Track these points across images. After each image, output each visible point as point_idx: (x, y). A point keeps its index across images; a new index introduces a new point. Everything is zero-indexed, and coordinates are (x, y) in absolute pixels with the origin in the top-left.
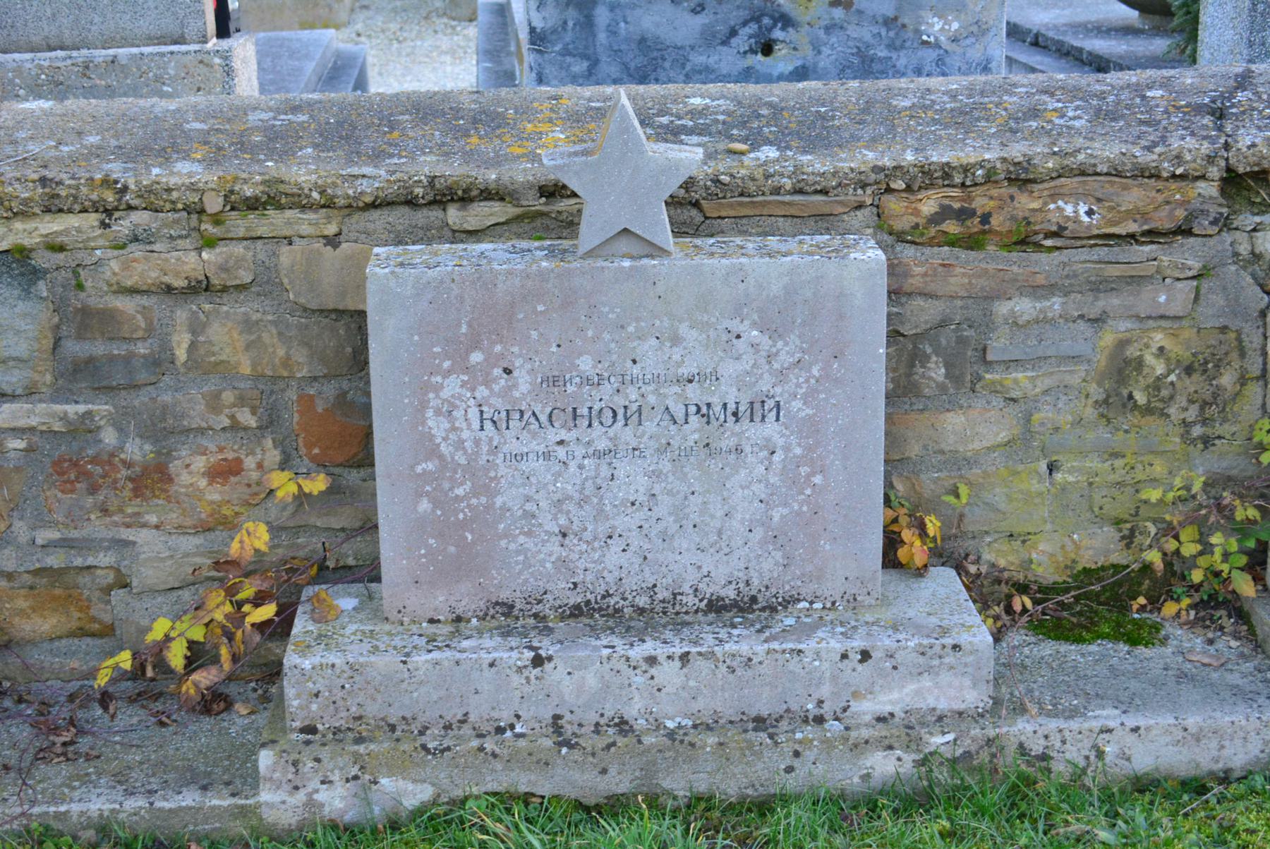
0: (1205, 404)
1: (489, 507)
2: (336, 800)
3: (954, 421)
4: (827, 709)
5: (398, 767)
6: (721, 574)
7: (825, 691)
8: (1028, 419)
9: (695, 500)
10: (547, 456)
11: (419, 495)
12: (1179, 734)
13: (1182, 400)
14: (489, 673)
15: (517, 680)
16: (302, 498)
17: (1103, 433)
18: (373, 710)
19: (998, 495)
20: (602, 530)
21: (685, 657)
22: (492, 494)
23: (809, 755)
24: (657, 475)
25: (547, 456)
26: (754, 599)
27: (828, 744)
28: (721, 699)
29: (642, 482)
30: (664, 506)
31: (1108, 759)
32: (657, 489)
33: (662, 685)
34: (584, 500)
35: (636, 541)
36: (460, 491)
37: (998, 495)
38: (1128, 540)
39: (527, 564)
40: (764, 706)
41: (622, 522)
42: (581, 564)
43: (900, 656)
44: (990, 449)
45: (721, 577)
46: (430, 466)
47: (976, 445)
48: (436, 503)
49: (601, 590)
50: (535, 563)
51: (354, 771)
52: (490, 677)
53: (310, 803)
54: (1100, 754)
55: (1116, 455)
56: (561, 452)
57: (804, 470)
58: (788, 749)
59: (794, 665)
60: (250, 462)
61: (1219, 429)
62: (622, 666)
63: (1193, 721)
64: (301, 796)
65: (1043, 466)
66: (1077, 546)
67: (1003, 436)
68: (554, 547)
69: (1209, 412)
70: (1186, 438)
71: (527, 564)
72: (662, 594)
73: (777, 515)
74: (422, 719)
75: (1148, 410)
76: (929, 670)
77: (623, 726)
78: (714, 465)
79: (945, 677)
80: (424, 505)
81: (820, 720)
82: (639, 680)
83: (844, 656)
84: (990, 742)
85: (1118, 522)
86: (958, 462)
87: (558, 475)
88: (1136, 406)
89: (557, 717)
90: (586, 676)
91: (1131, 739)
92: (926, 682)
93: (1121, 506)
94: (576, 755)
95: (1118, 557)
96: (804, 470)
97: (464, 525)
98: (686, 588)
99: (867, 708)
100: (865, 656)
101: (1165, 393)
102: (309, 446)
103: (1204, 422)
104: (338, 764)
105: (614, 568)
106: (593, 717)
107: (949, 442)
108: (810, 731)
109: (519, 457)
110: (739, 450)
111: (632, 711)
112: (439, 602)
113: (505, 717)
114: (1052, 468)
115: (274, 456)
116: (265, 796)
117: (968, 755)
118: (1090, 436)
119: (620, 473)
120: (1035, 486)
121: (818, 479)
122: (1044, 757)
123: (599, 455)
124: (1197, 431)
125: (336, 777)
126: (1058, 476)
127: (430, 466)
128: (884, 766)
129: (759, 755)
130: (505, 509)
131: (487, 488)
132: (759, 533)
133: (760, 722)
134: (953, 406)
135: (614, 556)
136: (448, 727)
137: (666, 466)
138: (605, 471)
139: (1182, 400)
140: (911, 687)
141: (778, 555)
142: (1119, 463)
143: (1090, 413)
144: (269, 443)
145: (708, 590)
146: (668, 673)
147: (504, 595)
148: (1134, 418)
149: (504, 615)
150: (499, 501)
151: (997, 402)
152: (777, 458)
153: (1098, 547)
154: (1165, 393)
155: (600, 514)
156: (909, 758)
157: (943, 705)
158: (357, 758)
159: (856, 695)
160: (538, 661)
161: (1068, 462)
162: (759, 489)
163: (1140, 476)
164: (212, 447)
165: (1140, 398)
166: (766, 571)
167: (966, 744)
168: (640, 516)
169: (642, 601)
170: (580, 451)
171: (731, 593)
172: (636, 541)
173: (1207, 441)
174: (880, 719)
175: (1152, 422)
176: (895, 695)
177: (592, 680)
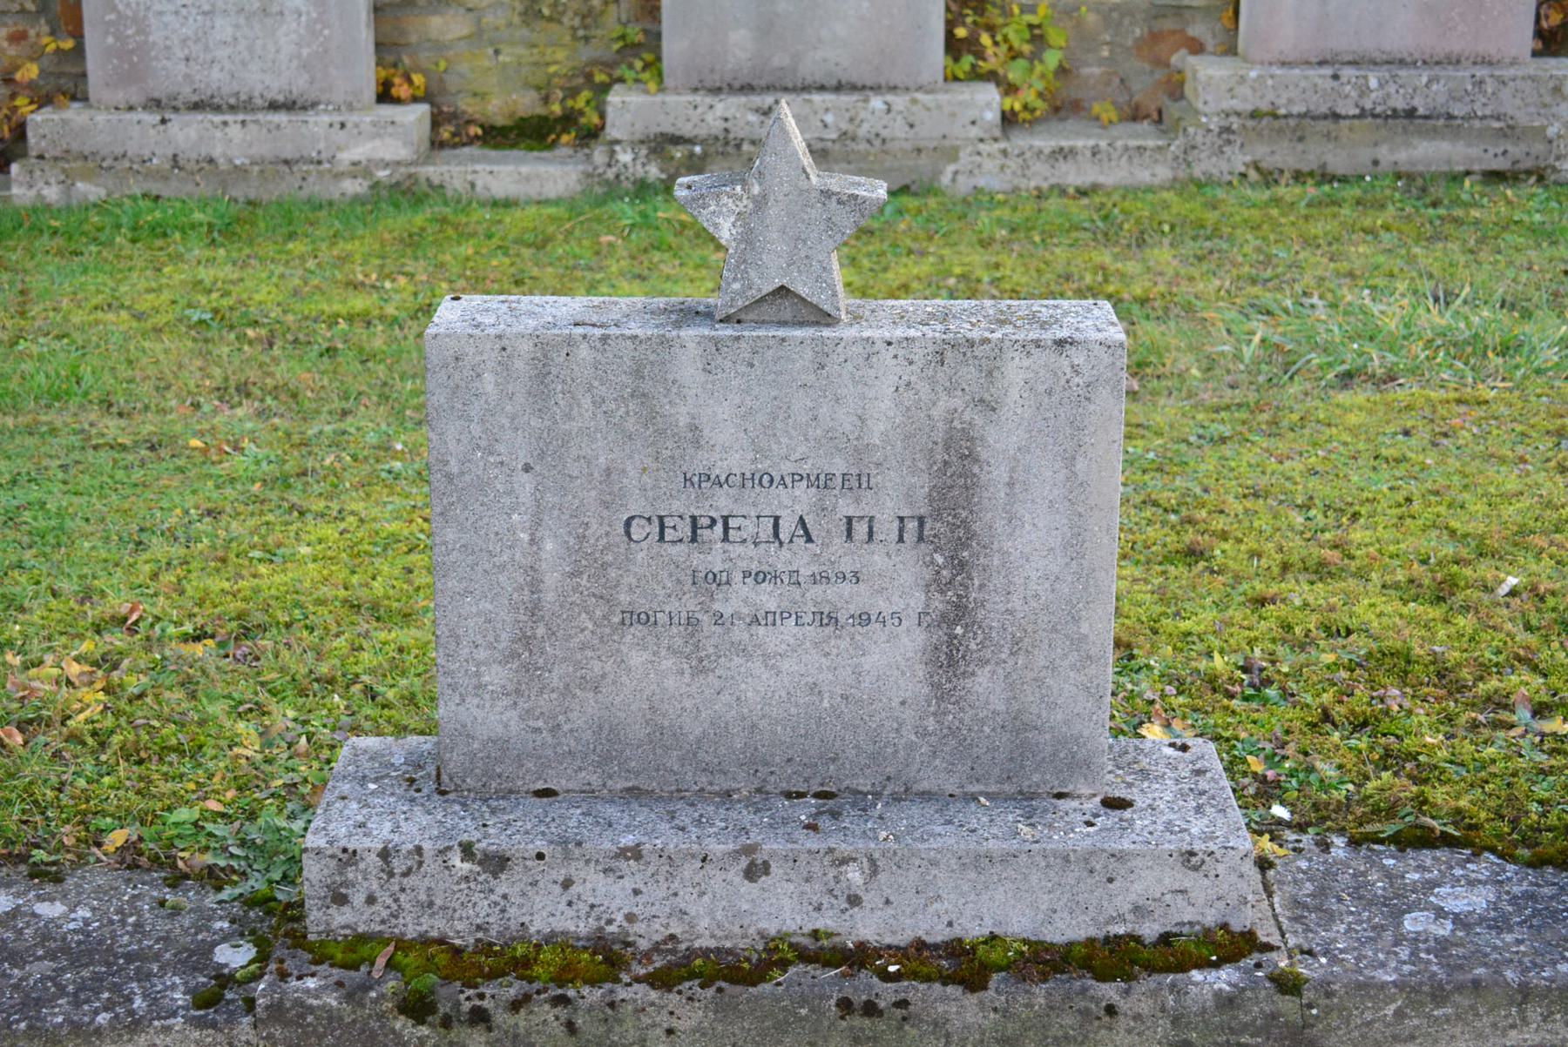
0: (584, 17)
1: (146, 42)
2: (52, 193)
3: (436, 22)
4: (324, 156)
5: (86, 176)
6: (275, 85)
7: (322, 145)
8: (479, 21)
9: (259, 42)
10: (177, 13)
11: (107, 33)
12: (516, 176)
13: (570, 14)
14: (137, 128)
15: (152, 132)
16: (58, 51)
17: (525, 32)
18: (75, 146)
19: (463, 67)
20: (209, 57)
21: (243, 122)
22: (147, 34)
23: (311, 179)
24: (237, 26)
25: (177, 13)
26: (294, 103)
27: (320, 174)
28: (263, 149)
29: (230, 30)
30: (242, 46)
31: (478, 189)
32: (238, 34)
33: (233, 141)
34: (197, 40)
35: (228, 66)
36: (130, 32)
37: (463, 67)
38: (546, 100)
39: (167, 77)
40: (288, 153)
41: (222, 53)
42: (198, 78)
43: (362, 126)
44: (460, 39)
45: (276, 87)
46: (113, 17)
47: (450, 36)
48: (117, 39)
49: (209, 93)
50: (171, 75)
51: (62, 177)
52: (142, 135)
53: (39, 195)
54: (473, 185)
55: (534, 46)
56: (184, 11)
57: (318, 27)
58: (298, 175)
59: (303, 129)
60: (32, 33)
61: (593, 32)
62: (209, 126)
63: (524, 169)
64: (32, 193)
65: (490, 51)
66: (515, 102)
67: (465, 32)
68: (182, 67)
69: (588, 21)
70: (575, 38)
71: (167, 77)
72: (243, 97)
73: (305, 52)
74: (102, 153)
75: (550, 19)
76: (378, 135)
77: (211, 161)
78: (269, 21)
79: (388, 140)
80: (110, 40)
81: (319, 162)
82: (218, 134)
83: (331, 125)
84: (410, 176)
85: (538, 88)
86: (440, 47)
87: (182, 25)
88: (543, 17)
89: (175, 156)
90: (187, 133)
91: (489, 177)
92: (377, 142)
93: (540, 78)
94: (183, 174)
95: (540, 110)
96: (318, 27)
97: (132, 52)
98: (256, 94)
99: (346, 157)
100: (343, 125)
101: (560, 9)
102: (67, 24)
103: (586, 27)
104: (54, 175)
105: (215, 79)
106: (194, 156)
107: (434, 34)
108: (311, 167)
109: (161, 13)
110: (282, 13)
111: (217, 152)
112: (120, 97)
113: (147, 154)
114: (497, 52)
115: (46, 29)
116: (15, 190)
117: (398, 184)
118: (518, 33)
119: (217, 25)
120: (487, 63)
121: (326, 32)
122: (442, 187)
123: (205, 13)
124: (581, 33)
125: (53, 180)
126: (501, 58)
127: (113, 17)
128: (352, 187)
129: (282, 178)
130: (154, 44)
131: (143, 30)
132: (295, 63)
133: (286, 162)
134: (435, 12)
135: (215, 74)
136: (116, 159)
137: (242, 21)
138: (208, 23)
139: (570, 14)
140: (369, 146)
141: (306, 77)
142: (535, 51)
143: (517, 20)
144: (43, 21)
145: (270, 96)
146: (235, 131)
147: (156, 95)
148: (543, 24)
149: (155, 104)
150: (151, 39)
151: (462, 11)
152: (303, 18)
153: (526, 103)
154: (560, 9)
155: (207, 49)
156: (366, 184)
157: (388, 157)
158: (64, 171)
159: (339, 148)
160: (163, 121)
161: (505, 49)
162: (294, 36)
163: (548, 59)
164: (10, 22)
165: (546, 11)
166: (300, 85)
167: (397, 177)
168: (229, 50)
169: (232, 101)
170: (194, 11)
171: (281, 98)
172: (228, 66)
173: (587, 39)
174: (354, 164)
175: (554, 26)
176: (360, 150)
177: (193, 133)
